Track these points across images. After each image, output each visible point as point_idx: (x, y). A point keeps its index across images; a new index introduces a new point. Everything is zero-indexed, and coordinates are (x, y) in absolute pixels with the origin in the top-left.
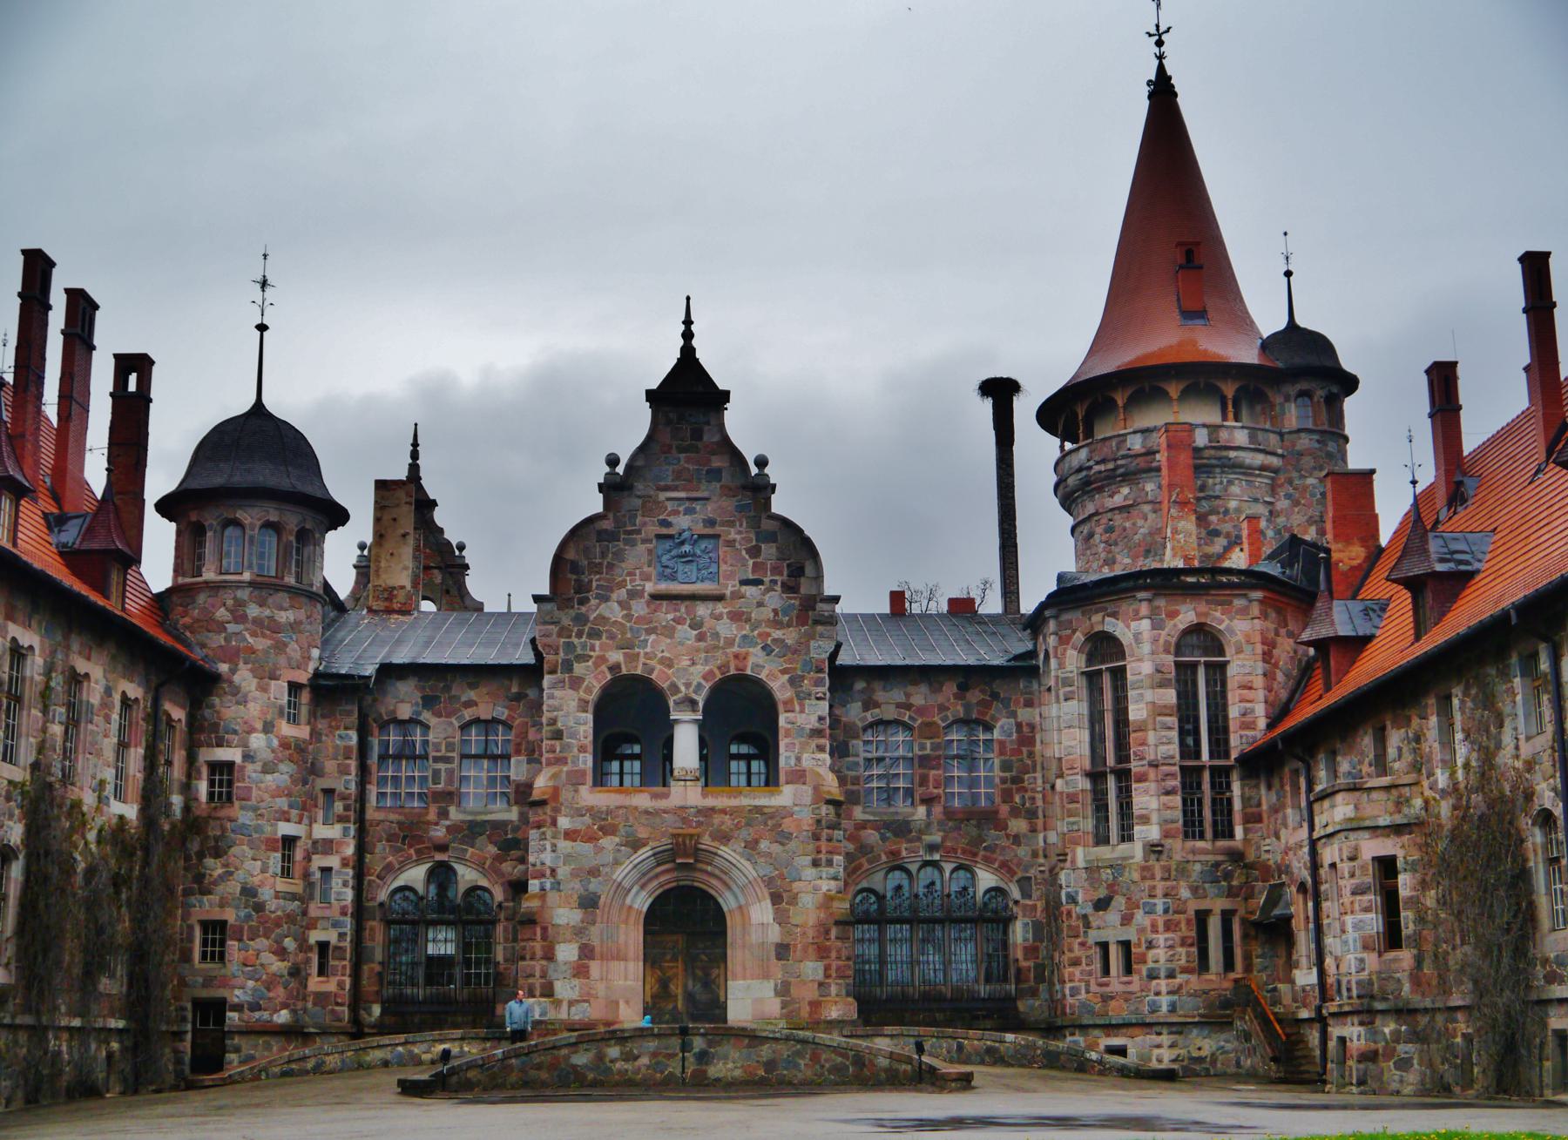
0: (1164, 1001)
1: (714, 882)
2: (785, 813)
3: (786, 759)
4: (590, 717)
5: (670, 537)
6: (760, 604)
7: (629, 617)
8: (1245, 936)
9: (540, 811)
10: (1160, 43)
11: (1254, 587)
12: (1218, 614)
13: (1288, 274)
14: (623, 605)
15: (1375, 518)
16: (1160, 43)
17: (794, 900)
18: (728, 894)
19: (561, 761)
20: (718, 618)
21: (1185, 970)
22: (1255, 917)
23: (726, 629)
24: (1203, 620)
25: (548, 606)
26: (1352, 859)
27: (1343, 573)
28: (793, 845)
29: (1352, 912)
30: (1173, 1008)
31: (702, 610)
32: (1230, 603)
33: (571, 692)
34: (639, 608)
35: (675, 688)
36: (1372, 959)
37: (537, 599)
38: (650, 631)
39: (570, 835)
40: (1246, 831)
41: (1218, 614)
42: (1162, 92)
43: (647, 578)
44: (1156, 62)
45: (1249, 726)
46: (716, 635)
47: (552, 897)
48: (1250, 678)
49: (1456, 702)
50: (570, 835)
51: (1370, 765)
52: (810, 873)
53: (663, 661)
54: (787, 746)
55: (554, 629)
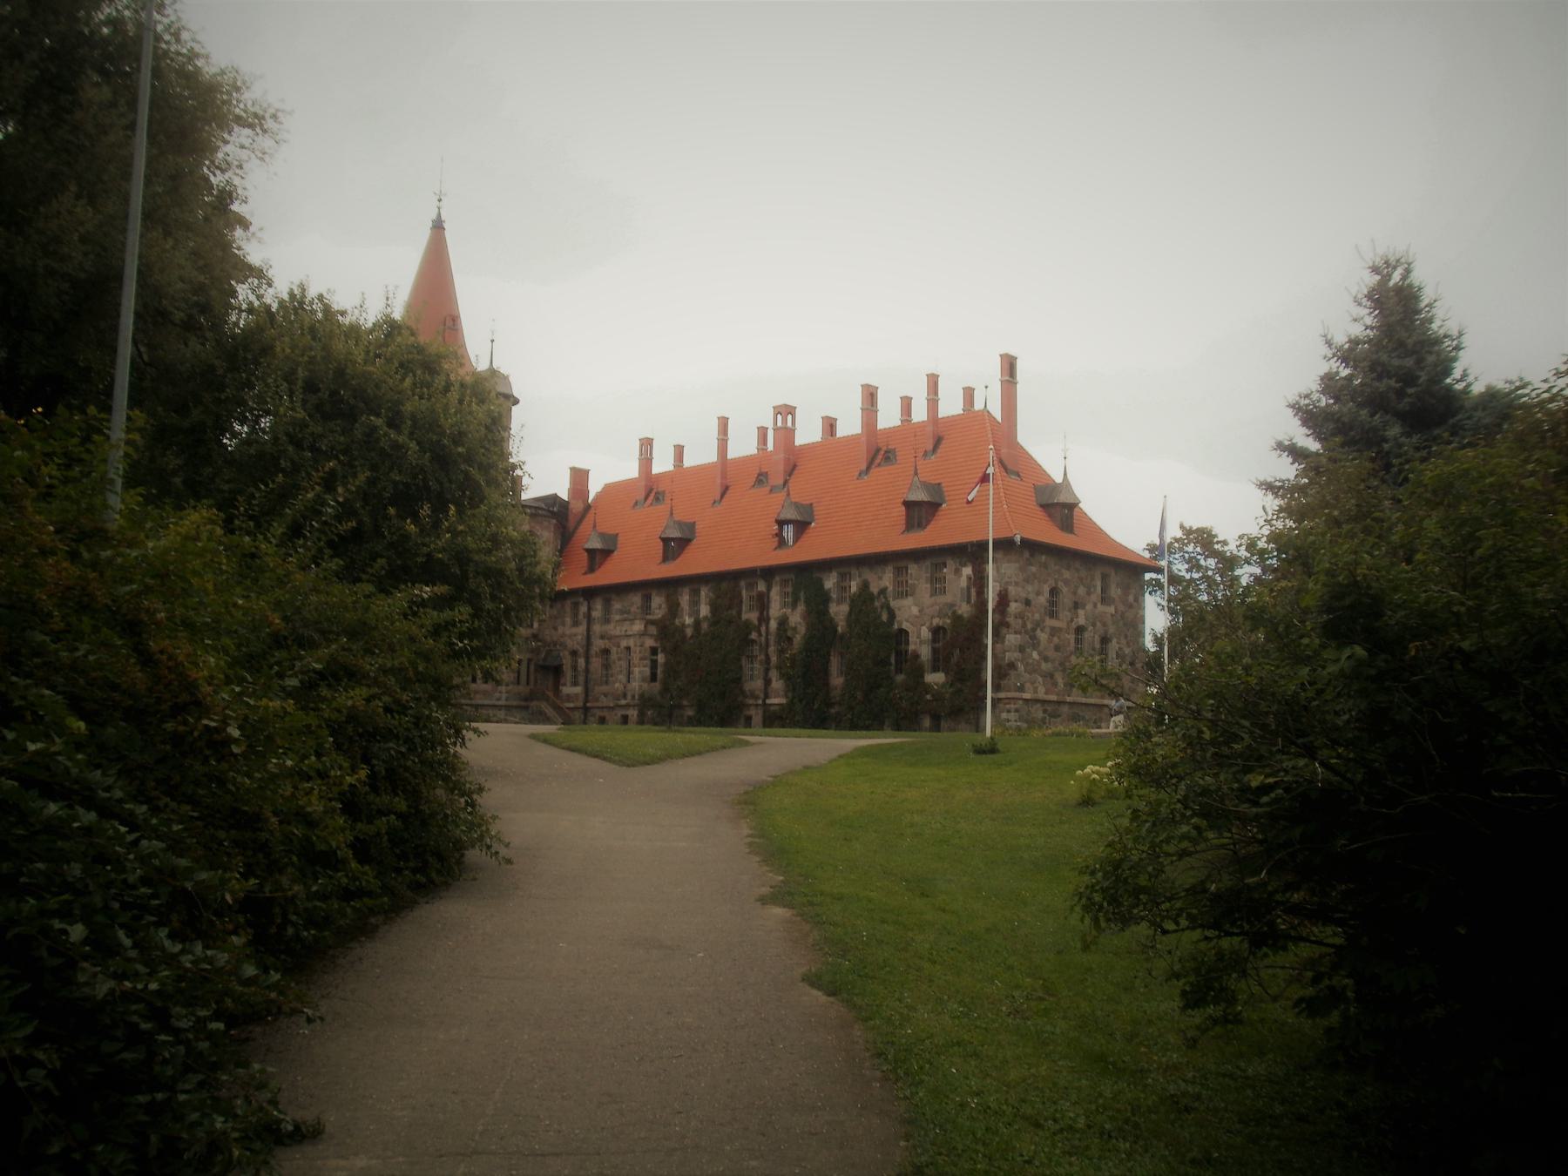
0: (504, 696)
8: (536, 671)
10: (440, 200)
11: (553, 519)
13: (492, 341)
16: (440, 200)
21: (512, 683)
22: (541, 663)
26: (641, 646)
29: (639, 666)
30: (506, 700)
36: (645, 686)
40: (540, 625)
42: (438, 226)
44: (437, 209)
51: (638, 608)
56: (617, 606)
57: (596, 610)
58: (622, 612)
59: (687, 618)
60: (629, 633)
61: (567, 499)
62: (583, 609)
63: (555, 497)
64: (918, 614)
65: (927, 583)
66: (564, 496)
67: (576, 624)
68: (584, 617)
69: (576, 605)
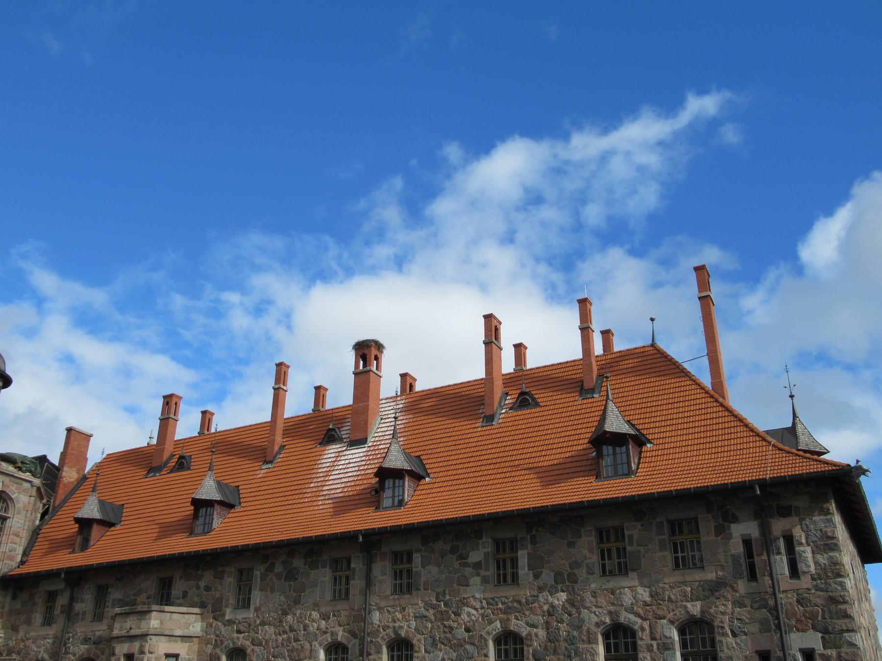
12: (14, 488)
15: (87, 459)
24: (5, 489)
27: (65, 486)
32: (21, 484)
41: (14, 488)
45: (11, 558)
48: (20, 530)
49: (257, 573)
56: (115, 594)
57: (83, 601)
58: (122, 603)
59: (228, 611)
60: (134, 632)
61: (57, 464)
62: (62, 600)
63: (43, 459)
64: (648, 599)
65: (661, 550)
66: (55, 459)
67: (48, 621)
68: (62, 612)
69: (52, 596)
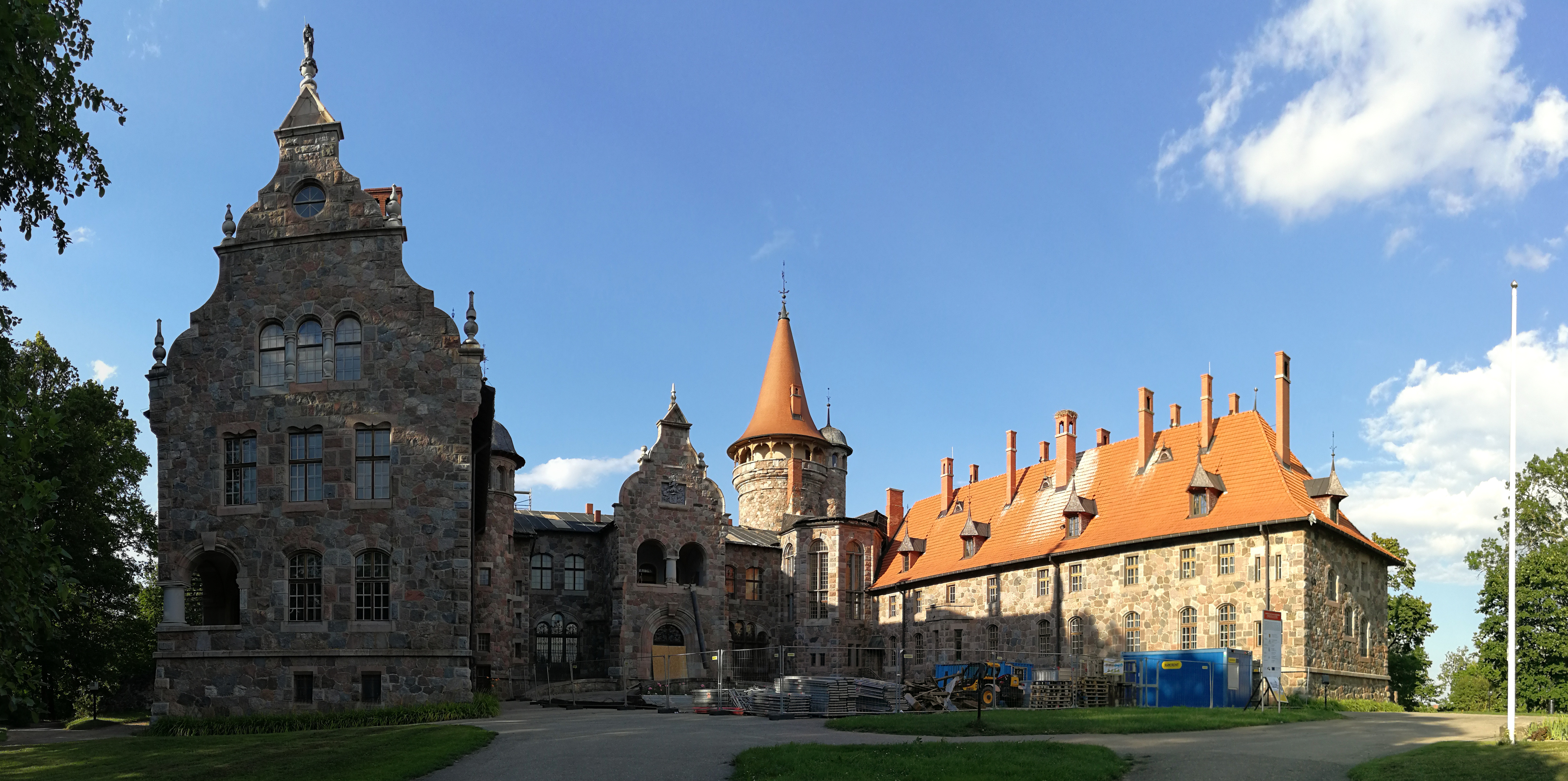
1: (681, 624)
2: (708, 598)
3: (709, 576)
4: (636, 555)
5: (668, 483)
6: (701, 515)
7: (651, 515)
9: (618, 591)
14: (649, 510)
17: (712, 632)
18: (686, 629)
19: (626, 573)
20: (685, 518)
23: (688, 523)
25: (622, 508)
28: (712, 611)
31: (679, 515)
33: (630, 545)
34: (655, 512)
35: (669, 546)
37: (614, 505)
38: (659, 522)
39: (628, 602)
43: (659, 500)
46: (685, 526)
47: (623, 628)
50: (628, 602)
52: (718, 622)
53: (664, 534)
54: (711, 573)
55: (622, 518)
